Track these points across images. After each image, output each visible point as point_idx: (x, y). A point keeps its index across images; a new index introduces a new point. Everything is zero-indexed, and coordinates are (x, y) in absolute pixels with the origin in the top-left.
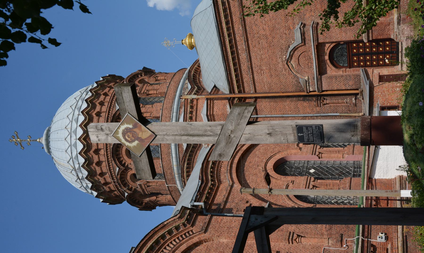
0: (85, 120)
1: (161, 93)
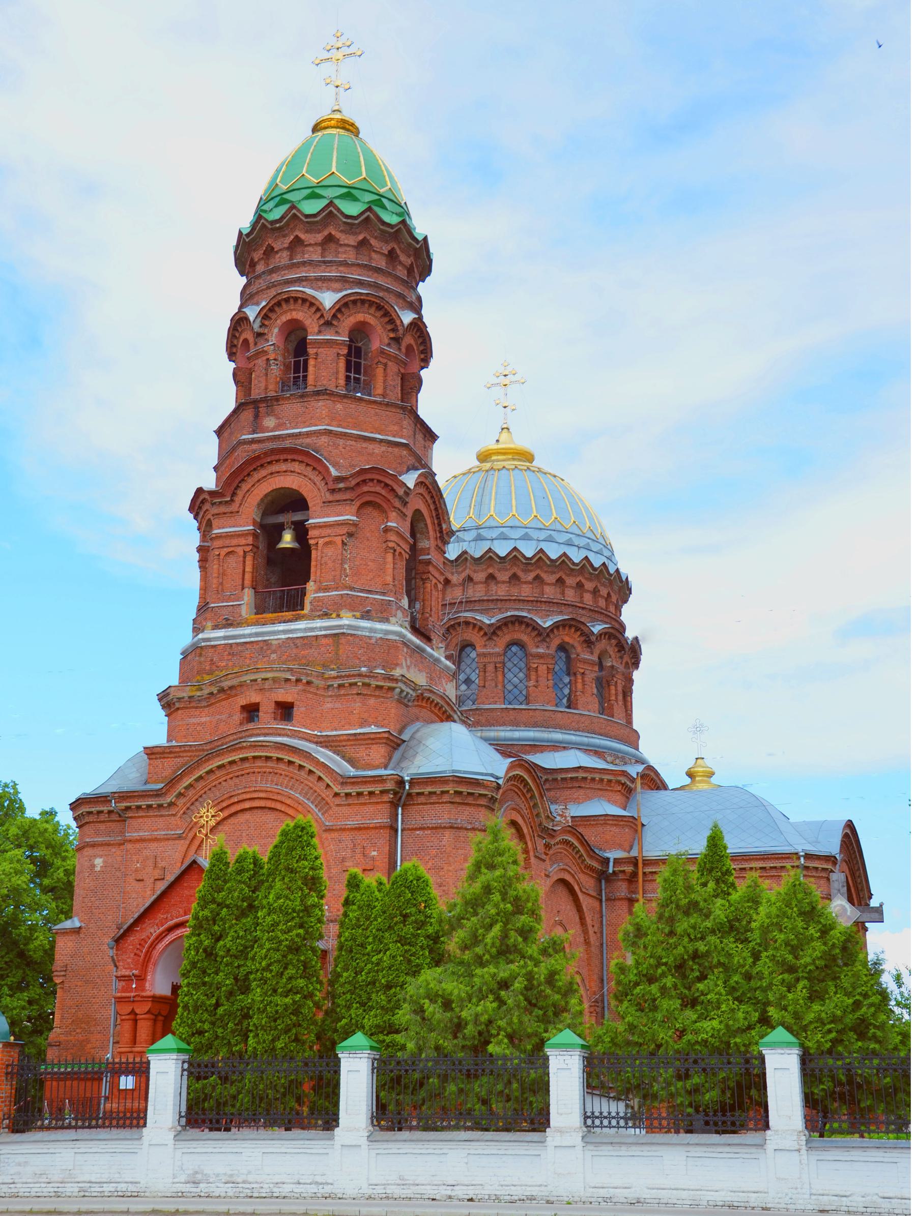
0: (574, 564)
1: (611, 707)
